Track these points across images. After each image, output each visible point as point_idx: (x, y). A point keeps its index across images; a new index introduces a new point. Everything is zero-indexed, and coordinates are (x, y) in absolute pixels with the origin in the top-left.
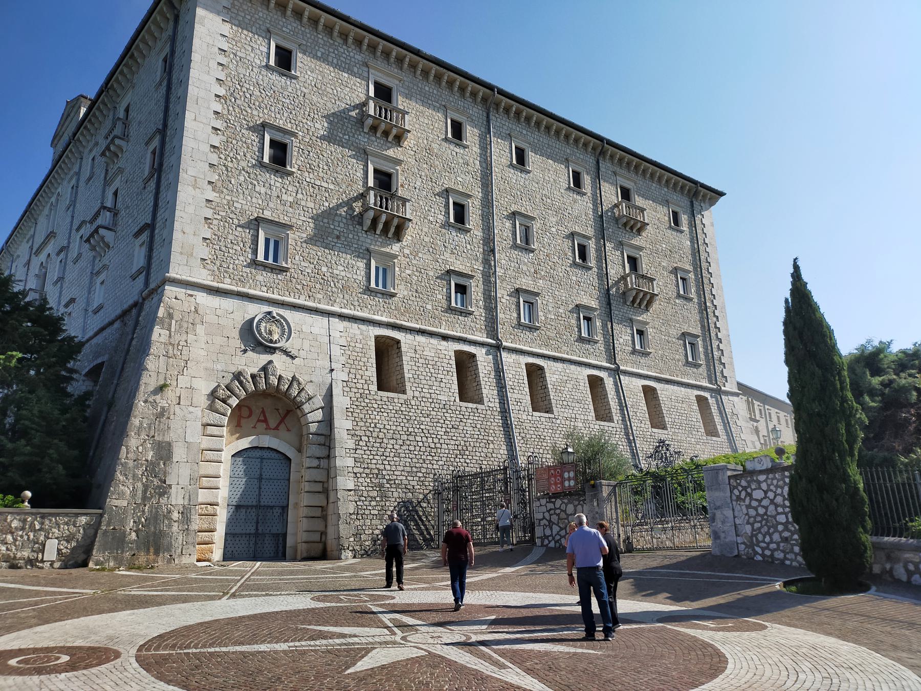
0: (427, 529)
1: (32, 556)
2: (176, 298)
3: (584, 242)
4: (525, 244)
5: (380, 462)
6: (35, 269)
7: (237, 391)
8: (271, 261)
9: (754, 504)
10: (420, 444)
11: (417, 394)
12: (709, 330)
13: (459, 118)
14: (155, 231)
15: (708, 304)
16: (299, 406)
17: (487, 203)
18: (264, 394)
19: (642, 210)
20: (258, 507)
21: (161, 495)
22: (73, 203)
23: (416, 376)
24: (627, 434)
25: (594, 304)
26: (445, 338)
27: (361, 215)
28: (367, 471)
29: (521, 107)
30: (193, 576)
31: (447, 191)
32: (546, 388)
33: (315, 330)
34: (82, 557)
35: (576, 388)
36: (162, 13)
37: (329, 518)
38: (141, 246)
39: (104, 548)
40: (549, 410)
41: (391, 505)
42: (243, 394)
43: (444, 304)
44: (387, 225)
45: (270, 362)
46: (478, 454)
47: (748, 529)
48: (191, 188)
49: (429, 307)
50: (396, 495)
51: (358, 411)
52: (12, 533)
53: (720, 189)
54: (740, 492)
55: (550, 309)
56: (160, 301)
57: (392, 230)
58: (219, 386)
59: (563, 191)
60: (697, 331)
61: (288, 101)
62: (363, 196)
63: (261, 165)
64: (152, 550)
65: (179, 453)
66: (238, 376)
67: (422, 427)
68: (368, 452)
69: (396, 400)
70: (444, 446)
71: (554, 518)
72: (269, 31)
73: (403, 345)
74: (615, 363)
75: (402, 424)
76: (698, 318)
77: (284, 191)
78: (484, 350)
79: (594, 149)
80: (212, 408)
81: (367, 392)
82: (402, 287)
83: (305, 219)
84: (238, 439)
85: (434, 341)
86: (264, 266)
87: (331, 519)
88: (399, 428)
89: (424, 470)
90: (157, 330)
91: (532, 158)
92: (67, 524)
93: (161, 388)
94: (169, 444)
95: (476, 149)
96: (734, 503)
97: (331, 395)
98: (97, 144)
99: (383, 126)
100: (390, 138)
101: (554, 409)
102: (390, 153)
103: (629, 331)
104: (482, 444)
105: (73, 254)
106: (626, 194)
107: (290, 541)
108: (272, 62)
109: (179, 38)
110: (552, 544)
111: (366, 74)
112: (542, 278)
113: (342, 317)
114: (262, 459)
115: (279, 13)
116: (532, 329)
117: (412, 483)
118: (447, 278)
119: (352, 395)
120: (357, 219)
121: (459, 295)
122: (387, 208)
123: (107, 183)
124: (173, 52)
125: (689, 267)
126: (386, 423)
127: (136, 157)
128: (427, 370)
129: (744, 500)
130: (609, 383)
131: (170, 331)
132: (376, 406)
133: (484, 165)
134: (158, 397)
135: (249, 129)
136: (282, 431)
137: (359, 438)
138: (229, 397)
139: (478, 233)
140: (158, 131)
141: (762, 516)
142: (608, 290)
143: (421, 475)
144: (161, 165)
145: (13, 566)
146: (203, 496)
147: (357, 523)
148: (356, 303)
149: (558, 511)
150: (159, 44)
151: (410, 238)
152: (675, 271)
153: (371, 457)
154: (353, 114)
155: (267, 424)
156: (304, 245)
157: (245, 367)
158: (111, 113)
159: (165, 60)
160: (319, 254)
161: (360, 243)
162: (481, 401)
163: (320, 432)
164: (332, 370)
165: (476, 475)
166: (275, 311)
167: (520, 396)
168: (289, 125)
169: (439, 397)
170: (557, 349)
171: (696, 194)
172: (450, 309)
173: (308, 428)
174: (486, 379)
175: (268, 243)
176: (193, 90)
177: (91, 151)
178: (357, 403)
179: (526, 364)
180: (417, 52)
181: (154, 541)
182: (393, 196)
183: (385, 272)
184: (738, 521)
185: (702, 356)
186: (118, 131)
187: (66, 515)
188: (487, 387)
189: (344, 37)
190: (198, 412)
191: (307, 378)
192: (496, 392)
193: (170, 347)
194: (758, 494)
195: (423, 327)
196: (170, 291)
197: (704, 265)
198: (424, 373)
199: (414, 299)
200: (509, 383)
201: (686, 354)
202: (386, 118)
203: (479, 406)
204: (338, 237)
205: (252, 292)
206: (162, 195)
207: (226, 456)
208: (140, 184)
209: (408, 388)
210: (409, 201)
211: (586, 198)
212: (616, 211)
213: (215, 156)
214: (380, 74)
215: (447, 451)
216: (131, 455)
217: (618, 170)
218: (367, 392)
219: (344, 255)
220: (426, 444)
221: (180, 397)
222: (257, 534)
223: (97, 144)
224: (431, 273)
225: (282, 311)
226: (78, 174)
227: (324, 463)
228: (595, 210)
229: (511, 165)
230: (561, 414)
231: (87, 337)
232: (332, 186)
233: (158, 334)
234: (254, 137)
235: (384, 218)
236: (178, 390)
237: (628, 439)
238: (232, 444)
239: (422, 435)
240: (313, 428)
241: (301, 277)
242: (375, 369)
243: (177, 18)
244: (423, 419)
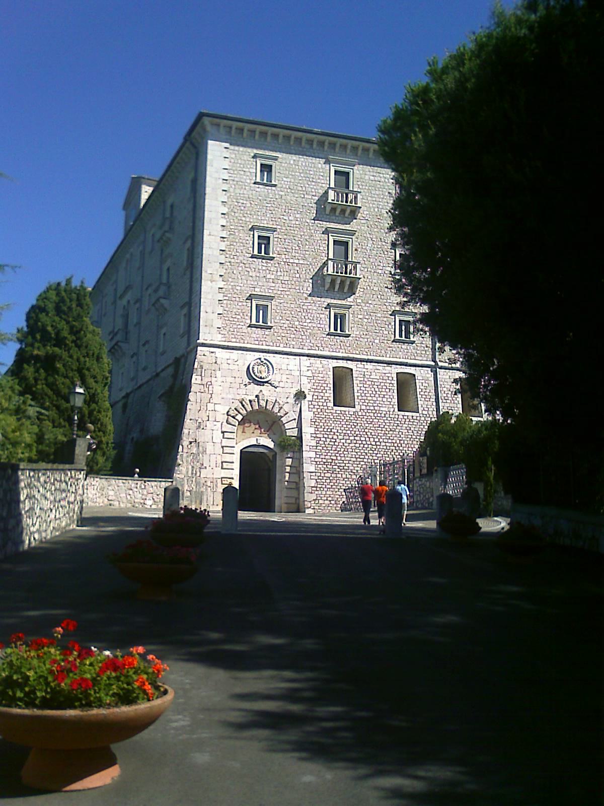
1: (142, 501)
2: (204, 355)
6: (120, 311)
7: (241, 411)
10: (364, 442)
11: (363, 407)
23: (363, 395)
26: (389, 363)
28: (324, 461)
42: (244, 412)
44: (342, 283)
48: (209, 282)
51: (319, 421)
52: (131, 489)
62: (325, 264)
67: (366, 430)
69: (347, 413)
70: (383, 444)
75: (351, 429)
77: (268, 271)
81: (326, 408)
83: (282, 289)
85: (380, 367)
87: (301, 492)
88: (349, 432)
90: (194, 377)
117: (356, 468)
119: (315, 410)
128: (373, 389)
131: (201, 375)
132: (332, 417)
137: (319, 439)
138: (237, 415)
147: (316, 492)
153: (327, 451)
168: (271, 223)
169: (381, 409)
186: (166, 227)
188: (423, 399)
189: (311, 142)
205: (249, 346)
206: (195, 284)
216: (185, 450)
218: (326, 408)
221: (208, 416)
225: (270, 357)
232: (301, 262)
233: (195, 379)
235: (338, 282)
239: (366, 436)
243: (197, 158)
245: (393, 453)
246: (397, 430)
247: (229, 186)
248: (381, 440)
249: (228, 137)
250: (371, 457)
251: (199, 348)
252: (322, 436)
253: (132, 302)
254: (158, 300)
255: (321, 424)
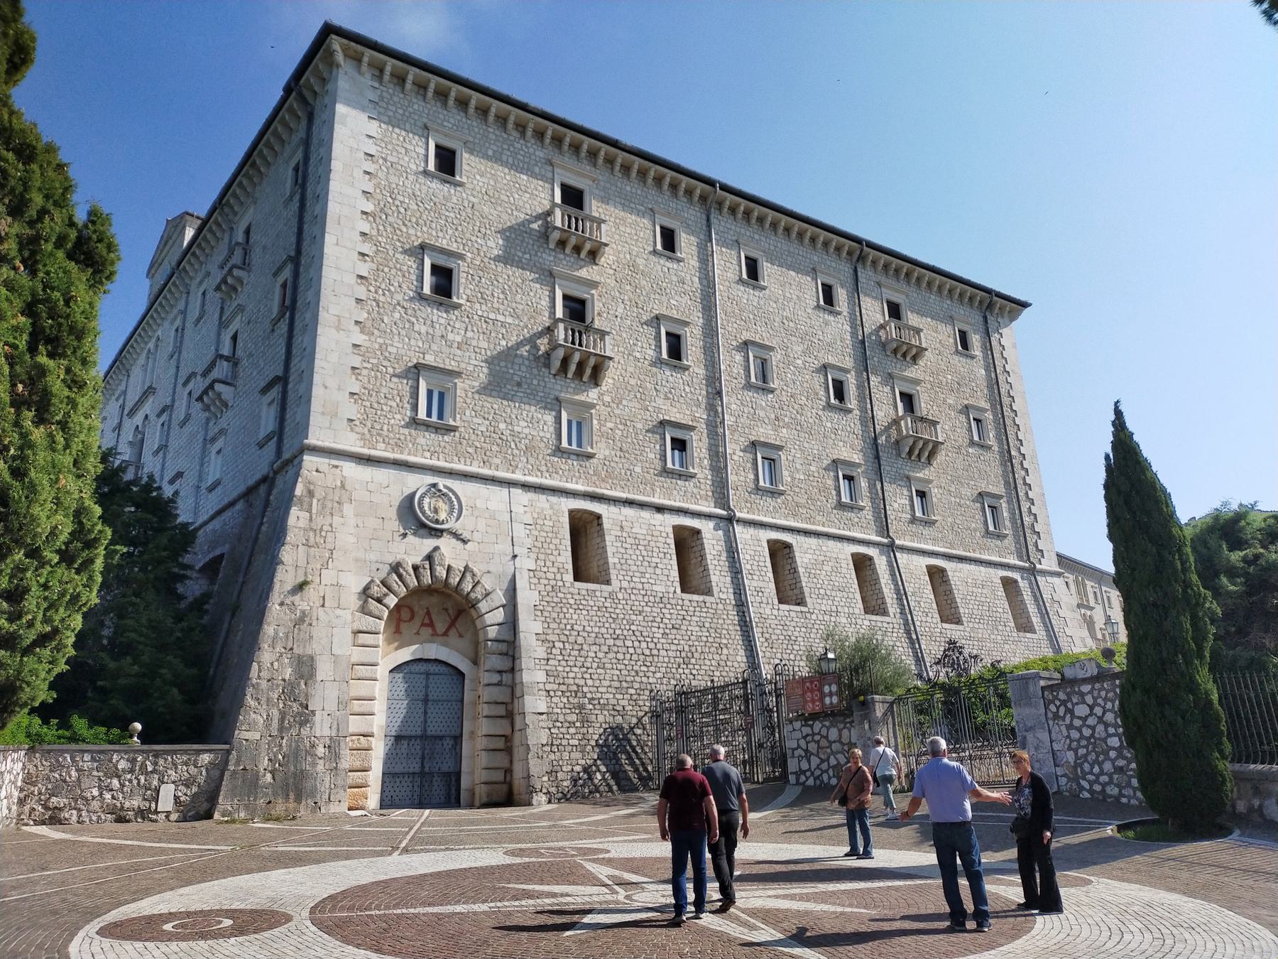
0: (643, 764)
3: (840, 376)
4: (762, 381)
5: (579, 675)
8: (434, 418)
9: (1077, 723)
10: (631, 651)
11: (625, 584)
12: (1016, 487)
13: (670, 224)
14: (288, 385)
15: (1013, 453)
16: (474, 605)
17: (710, 331)
18: (429, 591)
19: (918, 331)
20: (424, 737)
21: (302, 724)
22: (178, 349)
24: (908, 632)
25: (857, 458)
26: (660, 509)
27: (547, 355)
28: (563, 688)
29: (752, 205)
30: (348, 828)
31: (657, 318)
32: (795, 571)
33: (493, 505)
34: (205, 806)
35: (836, 570)
36: (291, 111)
37: (515, 751)
38: (270, 404)
39: (233, 793)
40: (801, 602)
41: (595, 733)
42: (403, 591)
43: (658, 465)
44: (581, 366)
45: (436, 549)
46: (708, 662)
47: (1070, 756)
48: (334, 330)
49: (638, 469)
50: (601, 718)
52: (119, 777)
53: (1023, 298)
54: (1058, 708)
55: (798, 466)
56: (297, 475)
57: (588, 371)
58: (372, 581)
59: (810, 311)
60: (999, 489)
61: (452, 215)
62: (549, 330)
63: (421, 297)
64: (292, 796)
65: (324, 670)
66: (396, 568)
67: (633, 628)
68: (563, 663)
69: (598, 594)
70: (663, 653)
71: (813, 747)
72: (426, 127)
73: (605, 520)
74: (888, 536)
76: (1000, 472)
78: (711, 524)
79: (850, 253)
80: (364, 610)
81: (560, 583)
82: (602, 445)
84: (397, 649)
85: (646, 514)
86: (427, 426)
87: (518, 753)
89: (636, 686)
90: (294, 512)
91: (768, 270)
92: (186, 764)
93: (301, 587)
94: (312, 658)
95: (694, 263)
96: (1051, 723)
97: (515, 590)
98: (208, 274)
99: (573, 241)
100: (583, 255)
101: (808, 600)
102: (584, 273)
103: (906, 492)
104: (712, 649)
105: (180, 413)
106: (895, 311)
107: (465, 782)
108: (431, 166)
109: (315, 141)
110: (811, 782)
111: (550, 175)
112: (787, 426)
113: (526, 486)
114: (428, 674)
115: (439, 104)
116: (775, 494)
118: (660, 430)
120: (542, 360)
121: (676, 452)
122: (580, 345)
123: (223, 325)
124: (306, 158)
125: (984, 404)
126: (586, 623)
127: (260, 293)
128: (638, 552)
129: (1063, 719)
130: (881, 563)
131: (310, 511)
132: (572, 601)
133: (705, 283)
134: (297, 598)
135: (405, 252)
136: (453, 637)
138: (386, 595)
139: (700, 371)
140: (290, 258)
141: (1088, 739)
142: (875, 439)
143: (633, 691)
144: (294, 301)
145: (121, 820)
146: (355, 724)
147: (552, 757)
148: (544, 468)
149: (817, 738)
150: (288, 149)
151: (610, 381)
152: (966, 409)
153: (568, 669)
154: (535, 226)
155: (434, 629)
156: (477, 396)
157: (405, 556)
158: (227, 237)
159: (296, 169)
160: (496, 406)
161: (547, 390)
162: (709, 592)
163: (501, 638)
164: (515, 557)
165: (705, 691)
166: (442, 482)
167: (761, 584)
168: (455, 245)
169: (655, 588)
170: (810, 520)
171: (990, 306)
172: (665, 472)
173: (486, 633)
174: (715, 562)
175: (431, 396)
176: (333, 208)
177: (201, 283)
178: (548, 599)
179: (768, 541)
180: (614, 144)
181: (295, 785)
182: (588, 329)
183: (580, 427)
184: (1056, 747)
185: (1008, 523)
186: (237, 258)
187: (186, 752)
188: (717, 573)
190: (347, 615)
191: (484, 568)
192: (729, 579)
193: (311, 534)
194: (1082, 710)
195: (631, 496)
196: (309, 460)
197: (1006, 400)
198: (634, 557)
199: (617, 459)
200: (746, 568)
201: (986, 521)
202: (576, 229)
203: (708, 599)
204: (519, 384)
205: (412, 459)
206: (297, 340)
207: (382, 671)
208: (267, 325)
209: (613, 577)
210: (608, 333)
211: (840, 319)
212: (882, 333)
213: (363, 288)
214: (568, 174)
215: (666, 660)
216: (264, 674)
217: (883, 279)
218: (560, 583)
219: (527, 407)
220: (639, 651)
222: (422, 774)
223: (208, 274)
224: (639, 426)
225: (450, 482)
226: (184, 313)
227: (506, 678)
228: (854, 334)
229: (741, 280)
230: (817, 606)
231: (200, 521)
232: (510, 320)
233: (296, 518)
234: (411, 263)
236: (322, 587)
237: (910, 638)
238: (390, 656)
239: (634, 638)
240: (492, 632)
241: (473, 437)
242: (570, 554)
243: (311, 118)
244: (634, 617)
245: (681, 671)
246: (684, 627)
247: (374, 166)
248: (659, 646)
249: (376, 85)
250: (644, 679)
251: (307, 458)
252: (555, 638)
253: (152, 417)
254: (211, 386)
255: (554, 615)
